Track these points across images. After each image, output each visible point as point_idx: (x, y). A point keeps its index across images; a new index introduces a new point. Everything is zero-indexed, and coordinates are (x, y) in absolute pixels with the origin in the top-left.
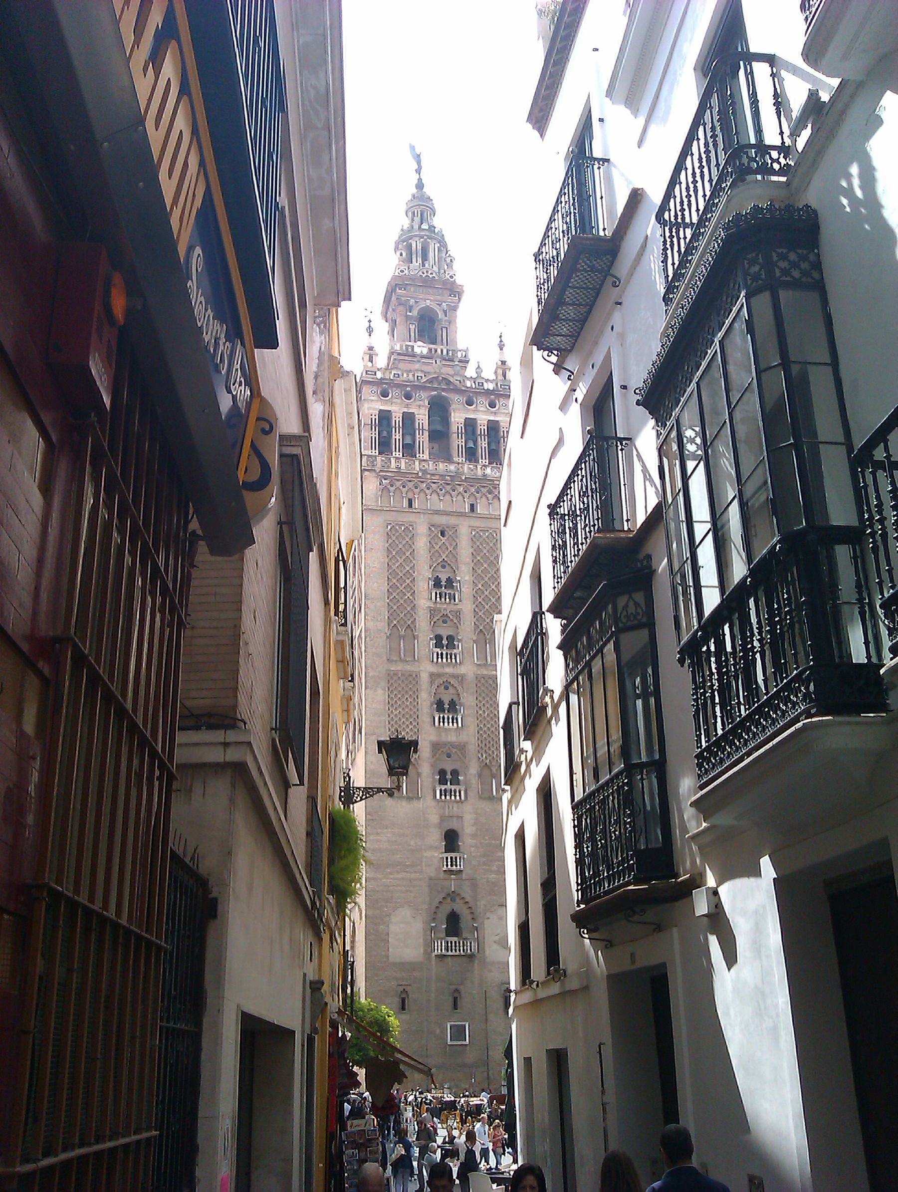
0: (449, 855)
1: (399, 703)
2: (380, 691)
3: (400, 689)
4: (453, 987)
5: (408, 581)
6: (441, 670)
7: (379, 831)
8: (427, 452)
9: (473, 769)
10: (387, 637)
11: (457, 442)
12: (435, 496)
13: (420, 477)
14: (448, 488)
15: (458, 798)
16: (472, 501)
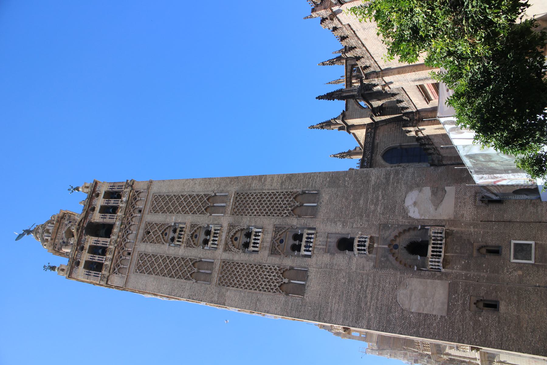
0: (356, 248)
1: (238, 279)
2: (228, 293)
3: (230, 276)
4: (475, 253)
5: (168, 261)
6: (223, 242)
7: (329, 310)
8: (108, 239)
9: (294, 221)
10: (196, 282)
11: (108, 219)
12: (130, 237)
13: (118, 245)
14: (127, 227)
15: (313, 236)
16: (137, 211)
